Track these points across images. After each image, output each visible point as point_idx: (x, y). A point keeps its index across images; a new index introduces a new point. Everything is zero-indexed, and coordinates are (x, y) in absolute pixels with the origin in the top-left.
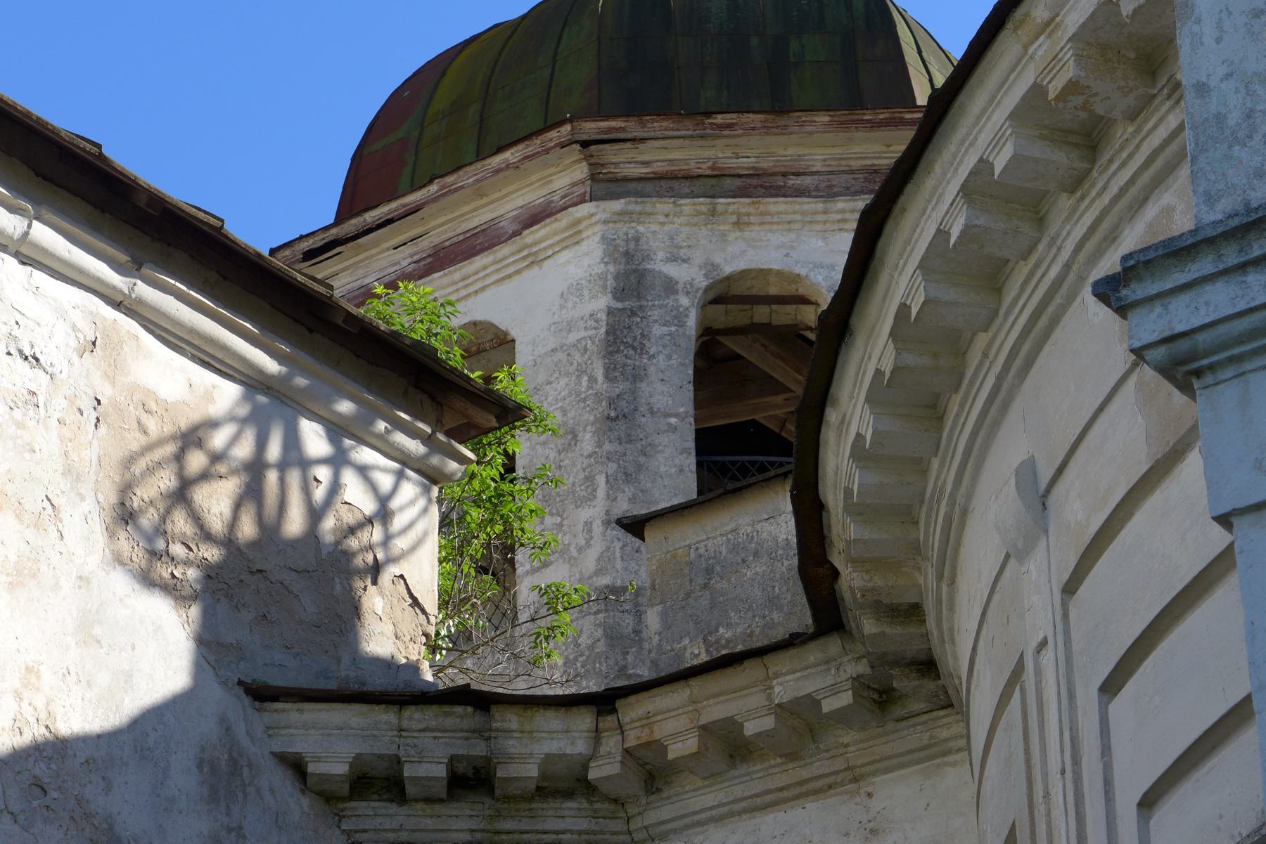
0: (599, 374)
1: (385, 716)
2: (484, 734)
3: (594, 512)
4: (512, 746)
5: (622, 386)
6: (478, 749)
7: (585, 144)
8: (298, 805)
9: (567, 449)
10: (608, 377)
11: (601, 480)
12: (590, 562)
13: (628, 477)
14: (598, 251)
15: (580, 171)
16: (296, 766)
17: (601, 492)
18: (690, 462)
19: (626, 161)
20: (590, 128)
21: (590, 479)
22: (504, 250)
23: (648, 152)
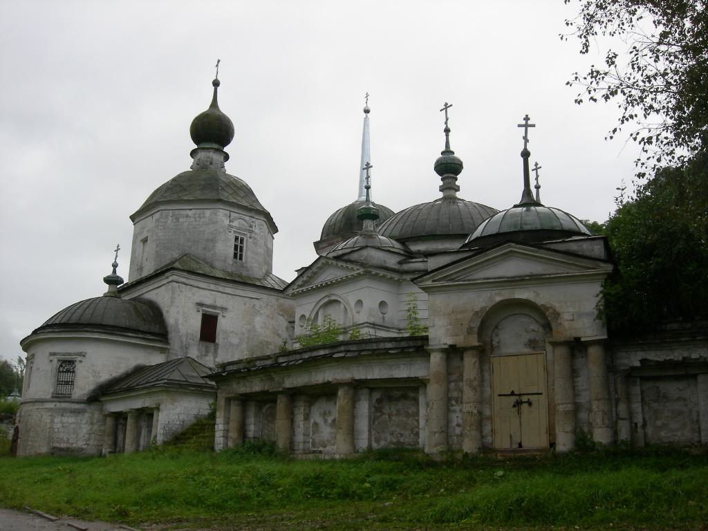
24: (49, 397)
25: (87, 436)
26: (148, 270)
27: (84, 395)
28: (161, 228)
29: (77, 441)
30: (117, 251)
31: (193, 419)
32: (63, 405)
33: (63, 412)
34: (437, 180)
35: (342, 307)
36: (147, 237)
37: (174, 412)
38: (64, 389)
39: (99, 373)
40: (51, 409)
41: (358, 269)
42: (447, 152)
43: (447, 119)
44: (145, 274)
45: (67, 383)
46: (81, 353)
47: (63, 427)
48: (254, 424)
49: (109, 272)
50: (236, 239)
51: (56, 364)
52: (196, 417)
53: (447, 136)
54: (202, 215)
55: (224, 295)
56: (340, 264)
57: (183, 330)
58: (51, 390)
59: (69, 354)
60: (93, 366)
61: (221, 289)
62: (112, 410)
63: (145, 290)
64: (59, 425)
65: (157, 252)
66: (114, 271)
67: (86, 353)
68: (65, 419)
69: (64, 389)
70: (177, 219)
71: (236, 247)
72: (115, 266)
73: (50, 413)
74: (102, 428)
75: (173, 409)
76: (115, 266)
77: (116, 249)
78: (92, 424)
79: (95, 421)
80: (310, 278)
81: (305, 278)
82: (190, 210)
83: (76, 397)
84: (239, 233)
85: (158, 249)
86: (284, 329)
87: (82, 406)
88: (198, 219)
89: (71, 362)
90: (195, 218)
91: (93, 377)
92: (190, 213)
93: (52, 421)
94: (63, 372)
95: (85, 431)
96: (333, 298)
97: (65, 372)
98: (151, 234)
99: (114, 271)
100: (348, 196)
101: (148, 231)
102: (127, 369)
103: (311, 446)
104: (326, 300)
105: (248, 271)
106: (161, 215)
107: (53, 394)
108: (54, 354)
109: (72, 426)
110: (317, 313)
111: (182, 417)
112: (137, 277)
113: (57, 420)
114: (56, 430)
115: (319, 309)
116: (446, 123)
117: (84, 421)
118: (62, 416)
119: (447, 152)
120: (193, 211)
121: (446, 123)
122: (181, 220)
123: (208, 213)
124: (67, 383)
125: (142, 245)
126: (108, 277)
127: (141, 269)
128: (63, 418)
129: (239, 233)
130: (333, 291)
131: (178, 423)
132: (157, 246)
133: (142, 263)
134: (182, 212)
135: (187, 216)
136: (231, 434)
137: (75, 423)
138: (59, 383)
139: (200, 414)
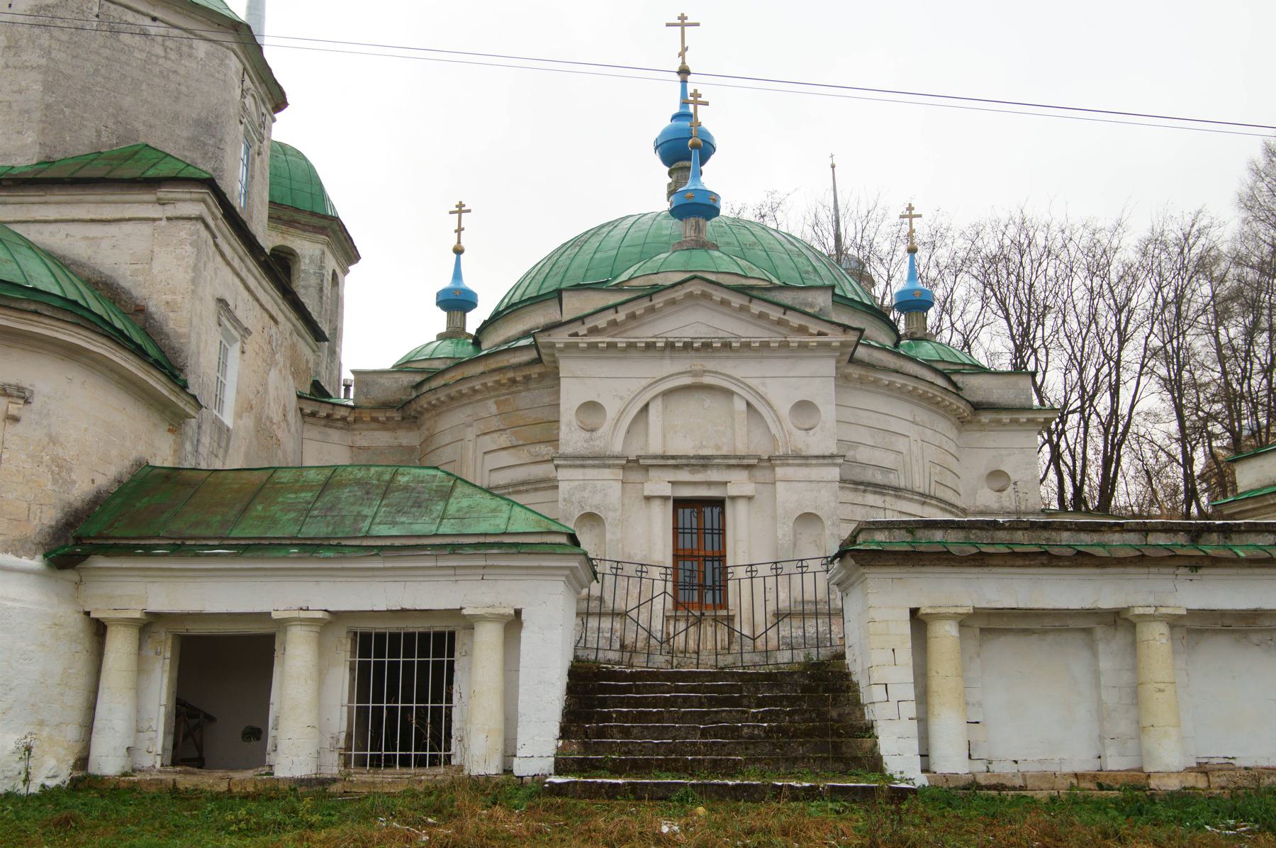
2: (333, 409)
4: (337, 412)
6: (331, 412)
34: (661, 175)
35: (740, 406)
39: (70, 470)
41: (820, 334)
43: (685, 49)
60: (53, 440)
65: (48, 107)
81: (621, 316)
82: (154, 19)
85: (50, 99)
91: (55, 482)
92: (154, 29)
104: (687, 380)
115: (655, 397)
116: (682, 54)
121: (682, 55)
123: (201, 48)
130: (711, 365)
132: (48, 88)
134: (130, 17)
135: (145, 34)
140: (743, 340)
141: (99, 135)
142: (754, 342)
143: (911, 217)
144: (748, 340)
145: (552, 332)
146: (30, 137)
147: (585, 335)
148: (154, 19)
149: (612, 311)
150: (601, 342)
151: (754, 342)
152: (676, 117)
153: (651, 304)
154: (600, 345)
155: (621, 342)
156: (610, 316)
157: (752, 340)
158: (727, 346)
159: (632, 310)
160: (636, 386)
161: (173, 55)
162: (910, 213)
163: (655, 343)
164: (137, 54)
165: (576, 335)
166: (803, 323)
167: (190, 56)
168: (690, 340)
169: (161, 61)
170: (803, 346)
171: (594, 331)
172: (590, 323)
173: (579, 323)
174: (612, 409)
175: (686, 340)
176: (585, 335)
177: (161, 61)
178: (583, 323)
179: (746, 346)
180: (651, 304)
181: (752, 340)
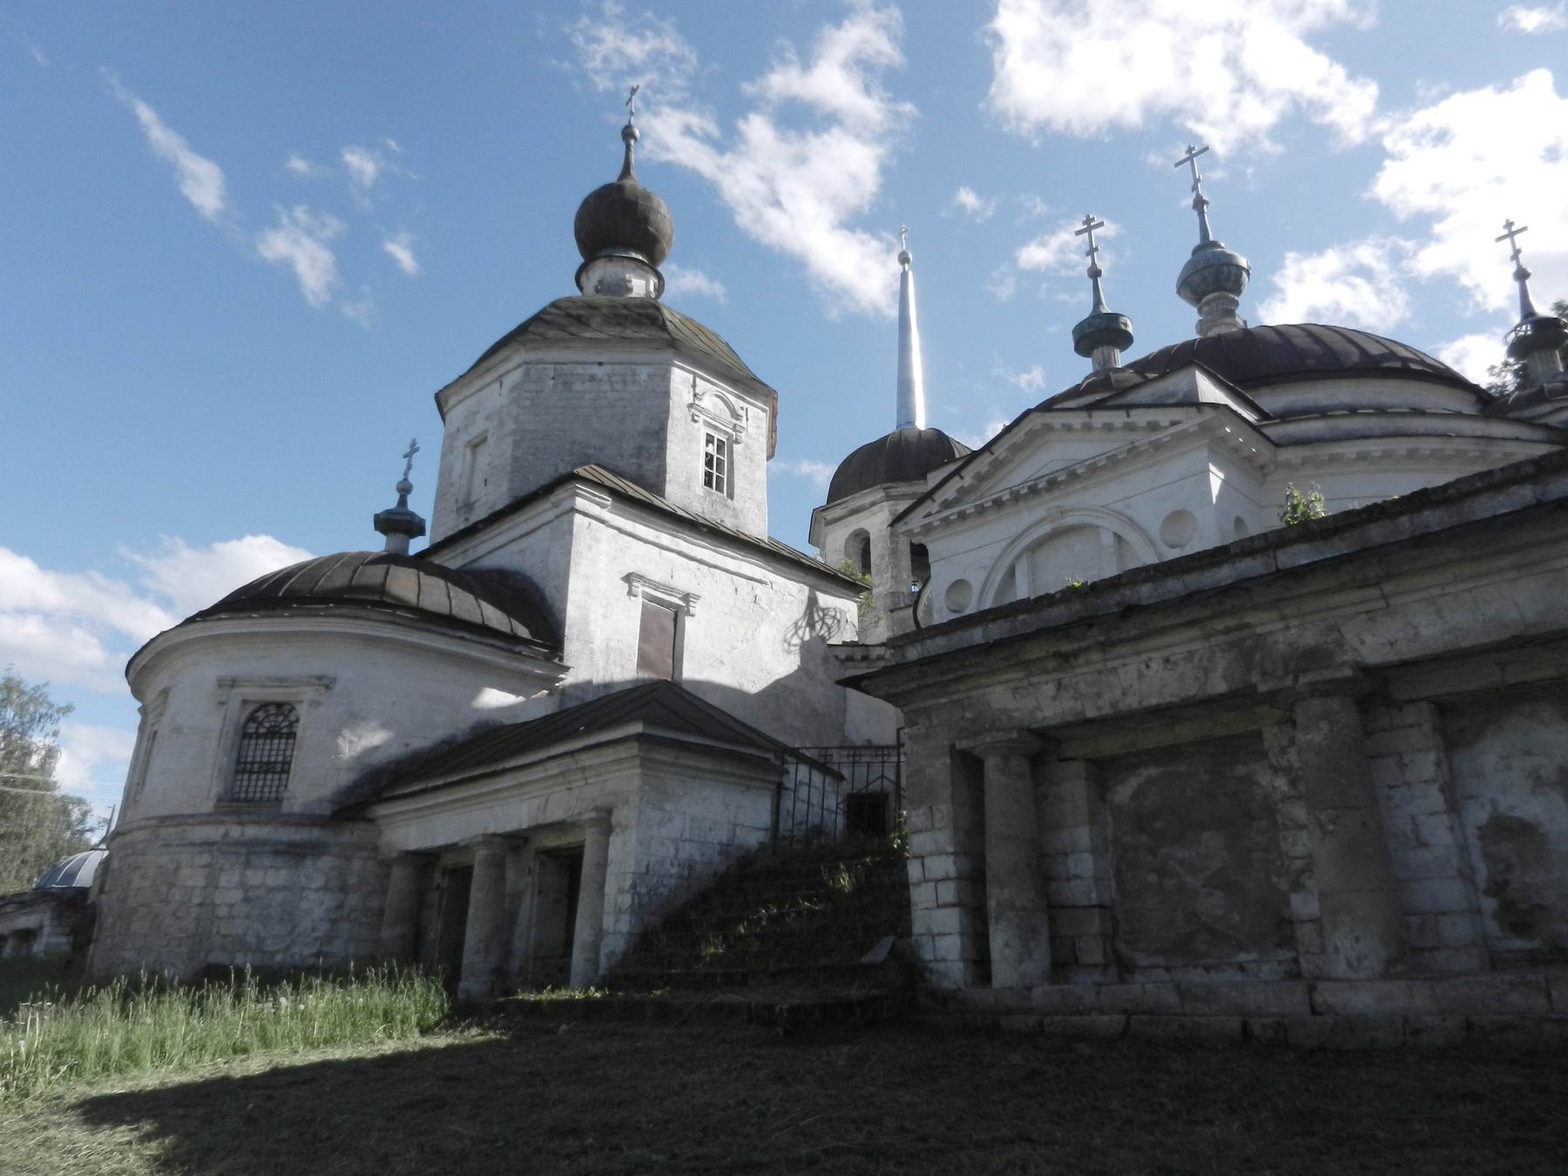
0: (889, 542)
1: (850, 649)
3: (888, 575)
5: (893, 546)
6: (866, 653)
7: (885, 489)
8: (837, 663)
9: (882, 560)
10: (891, 544)
11: (890, 567)
12: (888, 587)
13: (896, 567)
14: (888, 513)
15: (883, 494)
16: (836, 657)
17: (890, 570)
18: (910, 562)
19: (894, 492)
20: (885, 485)
21: (887, 568)
22: (866, 512)
23: (899, 489)
24: (208, 806)
25: (323, 928)
26: (493, 496)
27: (321, 800)
28: (527, 403)
29: (293, 943)
30: (408, 456)
31: (717, 859)
32: (252, 832)
33: (250, 851)
35: (1107, 540)
36: (486, 431)
37: (664, 832)
38: (260, 786)
40: (208, 844)
41: (1174, 424)
42: (1206, 244)
44: (480, 514)
45: (268, 768)
46: (320, 678)
47: (247, 900)
48: (1094, 851)
49: (391, 502)
50: (710, 440)
51: (236, 713)
52: (725, 849)
53: (1201, 214)
54: (629, 378)
55: (694, 564)
56: (1100, 418)
57: (599, 633)
58: (217, 789)
59: (282, 681)
61: (683, 545)
62: (412, 845)
63: (482, 550)
64: (236, 896)
65: (515, 459)
66: (403, 502)
67: (334, 680)
68: (254, 877)
69: (260, 786)
70: (568, 385)
71: (709, 463)
72: (405, 490)
73: (205, 859)
74: (374, 903)
75: (661, 824)
76: (405, 490)
77: (408, 450)
78: (343, 889)
79: (352, 880)
80: (980, 478)
82: (600, 364)
83: (297, 809)
84: (715, 428)
85: (519, 453)
86: (819, 661)
87: (315, 834)
88: (618, 387)
89: (283, 708)
90: (611, 383)
92: (599, 372)
93: (212, 884)
94: (258, 736)
95: (318, 912)
96: (1070, 520)
97: (265, 736)
98: (496, 422)
99: (403, 502)
100: (880, 426)
101: (488, 418)
102: (451, 732)
103: (1493, 928)
104: (1046, 528)
105: (736, 517)
106: (527, 374)
107: (220, 800)
108: (233, 683)
109: (279, 897)
110: (1011, 572)
111: (687, 851)
112: (454, 524)
113: (229, 879)
114: (222, 911)
115: (1019, 556)
116: (1195, 188)
117: (319, 881)
118: (247, 865)
119: (1206, 244)
120: (607, 369)
122: (578, 387)
124: (268, 768)
125: (468, 452)
126: (388, 512)
127: (468, 506)
128: (249, 873)
129: (715, 428)
130: (1068, 502)
131: (674, 870)
132: (516, 445)
133: (469, 493)
134: (580, 369)
135: (593, 379)
136: (996, 896)
137: (285, 888)
138: (242, 767)
139: (737, 842)
140: (1087, 463)
141: (556, 466)
142: (1100, 461)
143: (1511, 234)
144: (1092, 461)
145: (908, 519)
146: (505, 486)
147: (939, 512)
148: (600, 364)
149: (957, 478)
150: (951, 515)
151: (1100, 461)
152: (1196, 251)
153: (993, 457)
154: (952, 518)
155: (969, 507)
156: (956, 484)
157: (1097, 459)
158: (1073, 476)
159: (976, 471)
160: (996, 550)
161: (618, 387)
162: (1510, 230)
163: (1000, 498)
164: (587, 396)
165: (929, 514)
166: (1150, 418)
167: (634, 382)
168: (1033, 483)
169: (609, 394)
170: (1157, 446)
171: (947, 505)
172: (940, 497)
173: (929, 502)
174: (976, 585)
175: (1029, 484)
176: (939, 512)
177: (609, 394)
178: (934, 501)
179: (1094, 469)
180: (993, 457)
181: (1097, 459)
